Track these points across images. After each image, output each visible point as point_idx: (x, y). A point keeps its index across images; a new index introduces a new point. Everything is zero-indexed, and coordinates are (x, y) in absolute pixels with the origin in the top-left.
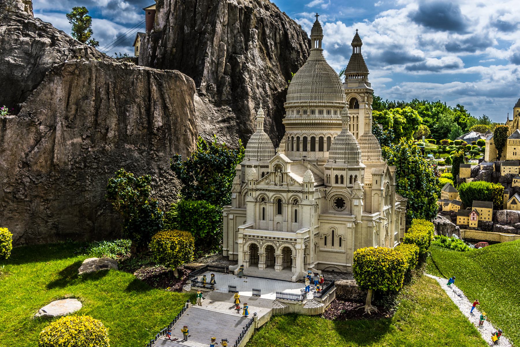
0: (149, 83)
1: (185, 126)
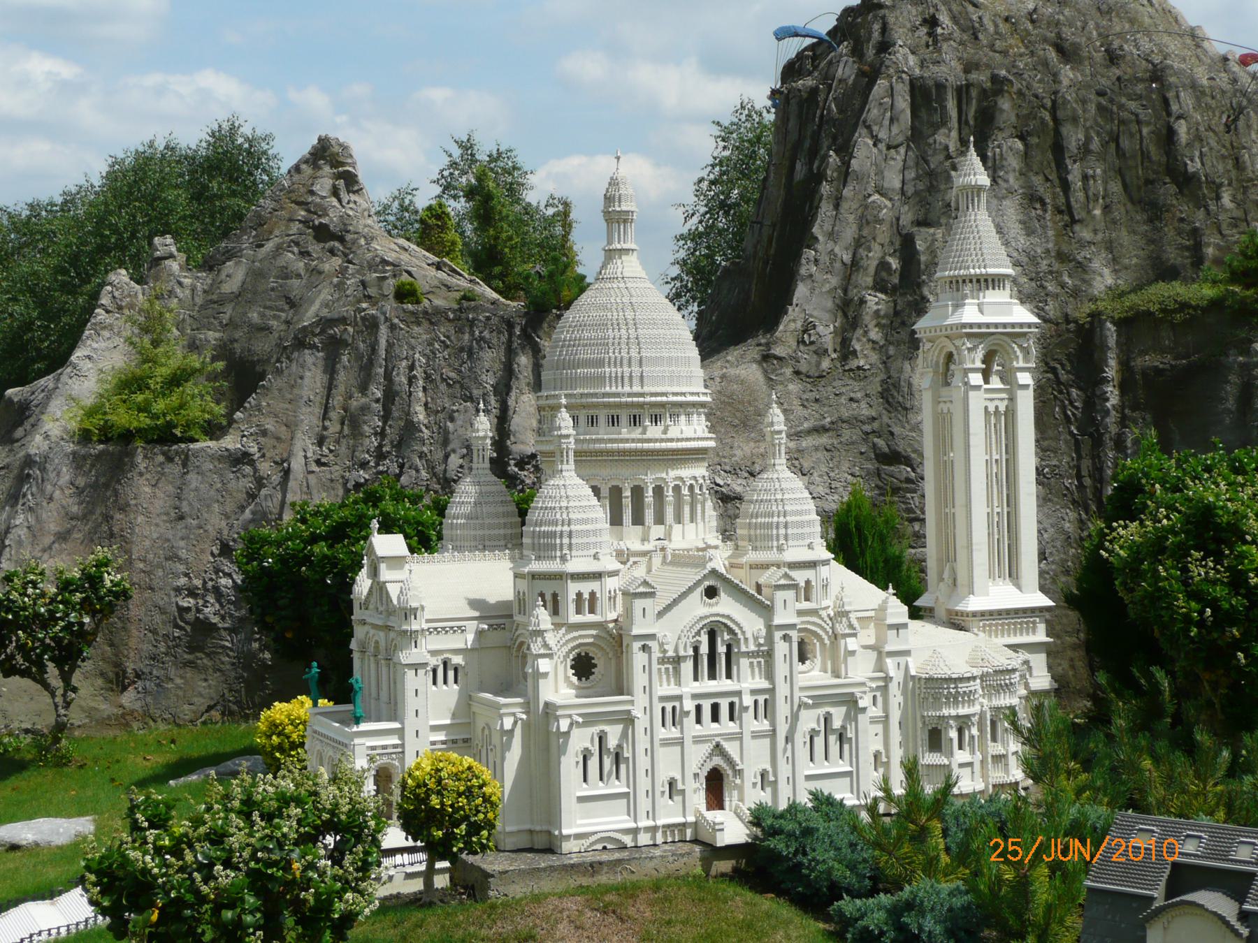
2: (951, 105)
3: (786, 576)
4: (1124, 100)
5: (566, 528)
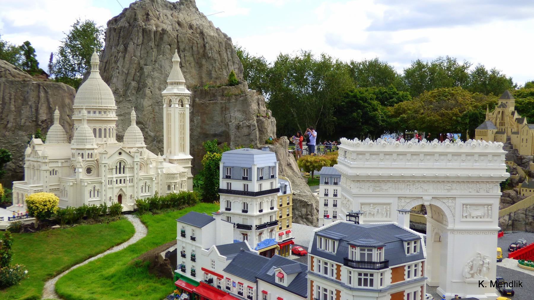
0: (39, 92)
1: (63, 120)
2: (153, 36)
3: (137, 150)
4: (194, 38)
5: (135, 137)
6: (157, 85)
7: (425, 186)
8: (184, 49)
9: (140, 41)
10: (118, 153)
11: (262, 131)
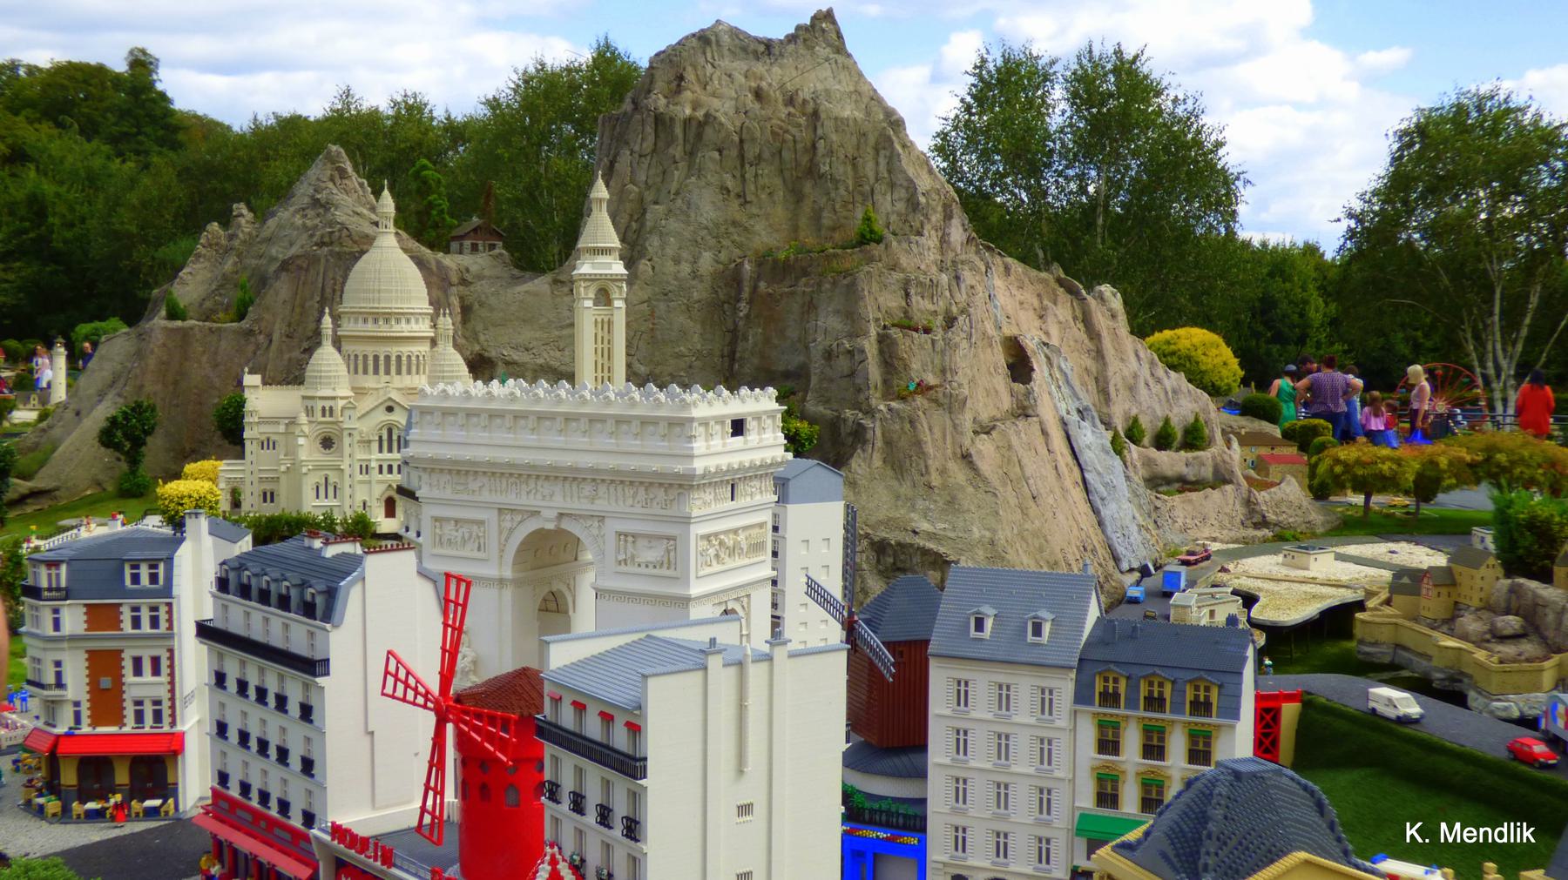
2: (678, 130)
6: (669, 251)
7: (546, 488)
8: (759, 158)
9: (648, 145)
10: (383, 408)
11: (892, 365)
